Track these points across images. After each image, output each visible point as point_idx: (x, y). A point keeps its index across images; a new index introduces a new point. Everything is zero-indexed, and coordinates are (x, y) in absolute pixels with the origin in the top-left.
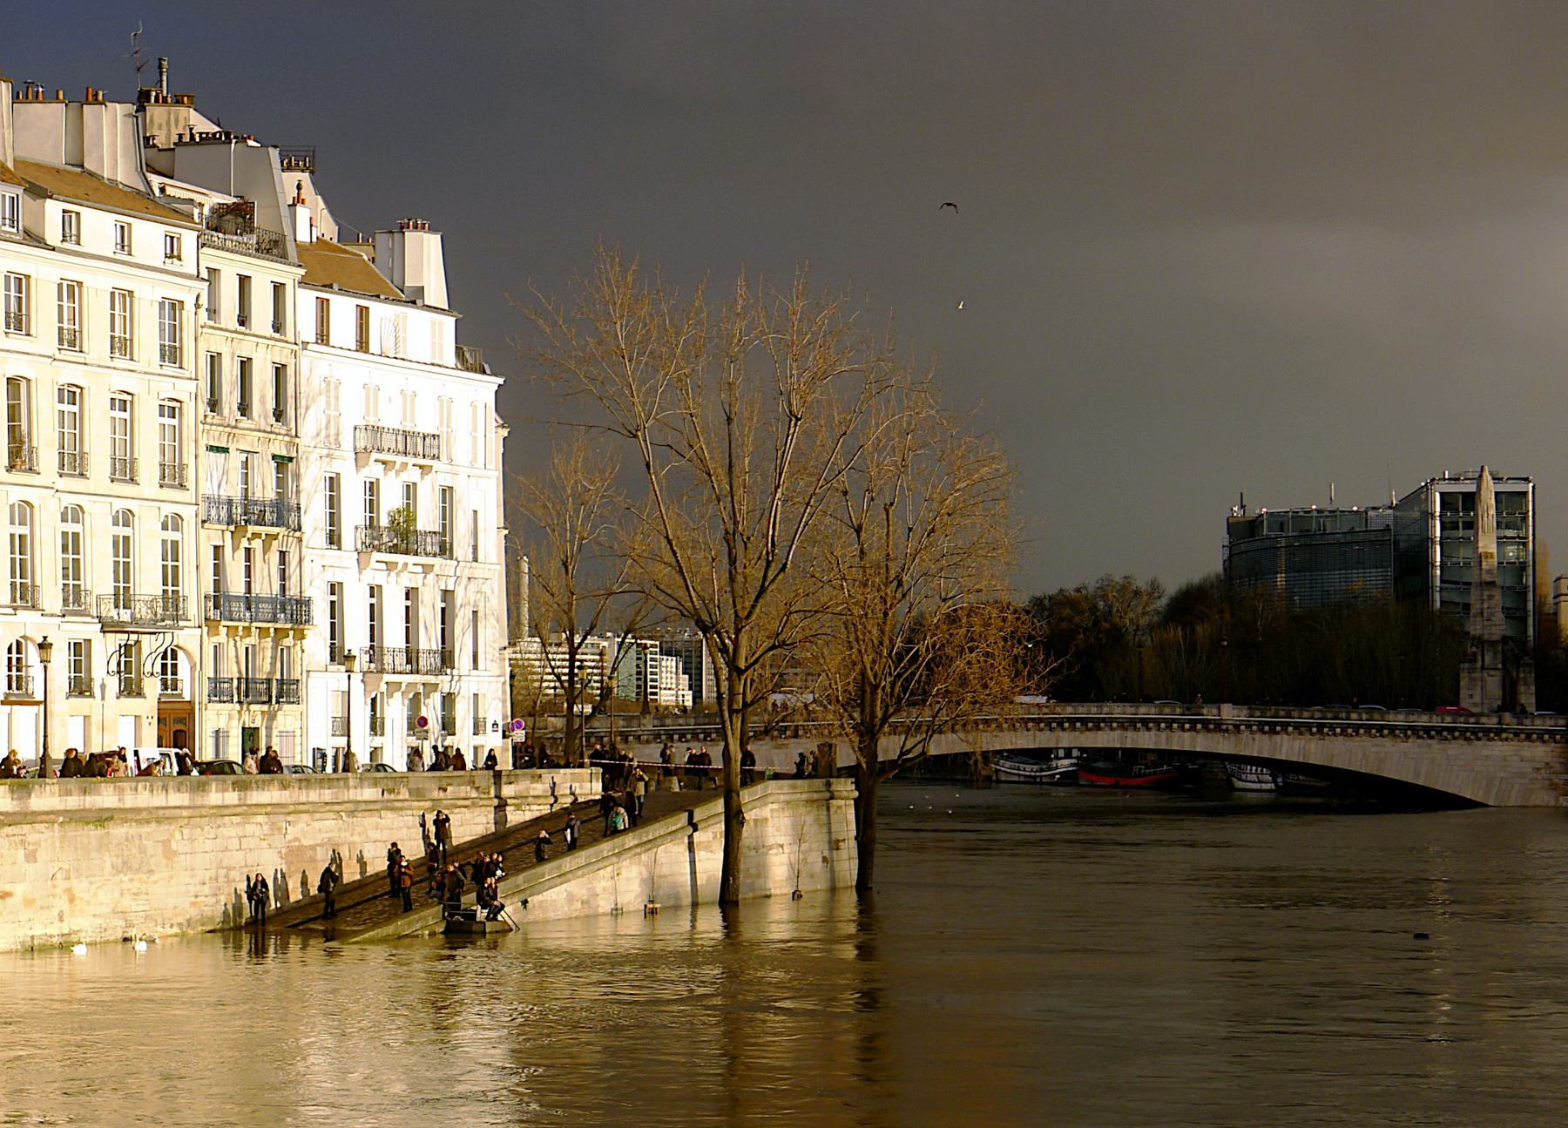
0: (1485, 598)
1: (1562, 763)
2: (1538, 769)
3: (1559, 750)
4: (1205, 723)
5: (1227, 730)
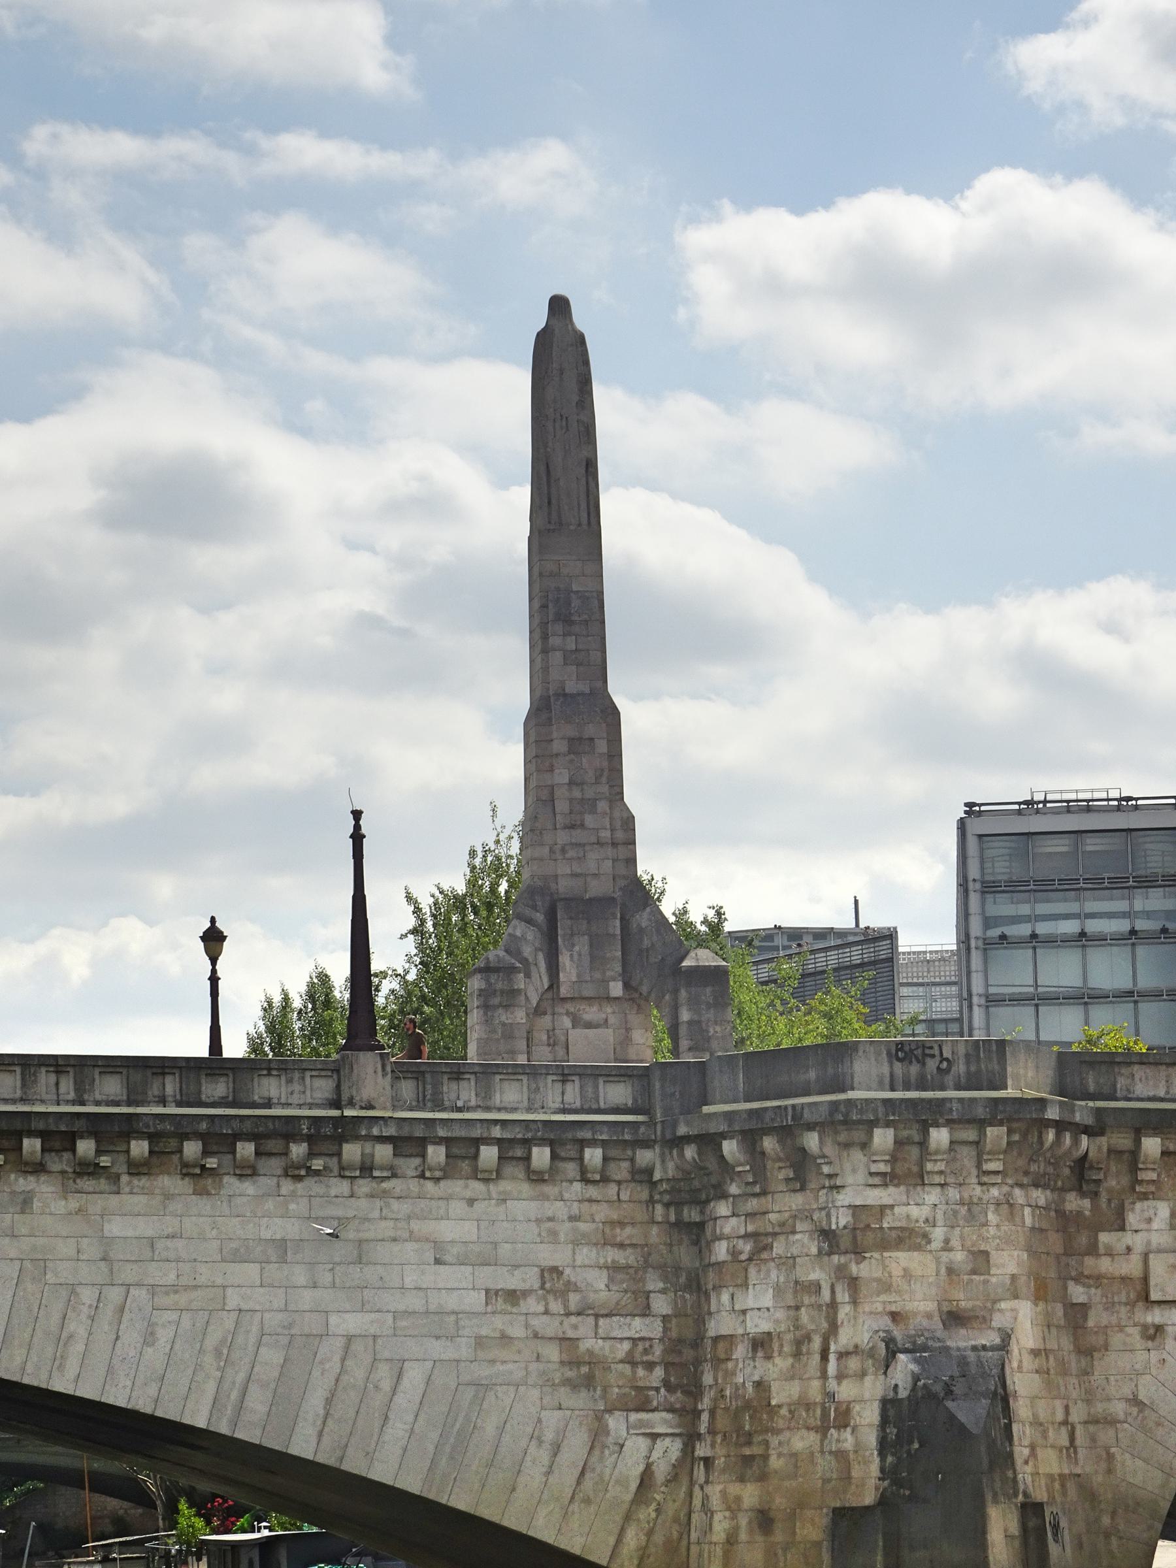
0: (559, 746)
1: (614, 1269)
2: (513, 1296)
3: (602, 1212)
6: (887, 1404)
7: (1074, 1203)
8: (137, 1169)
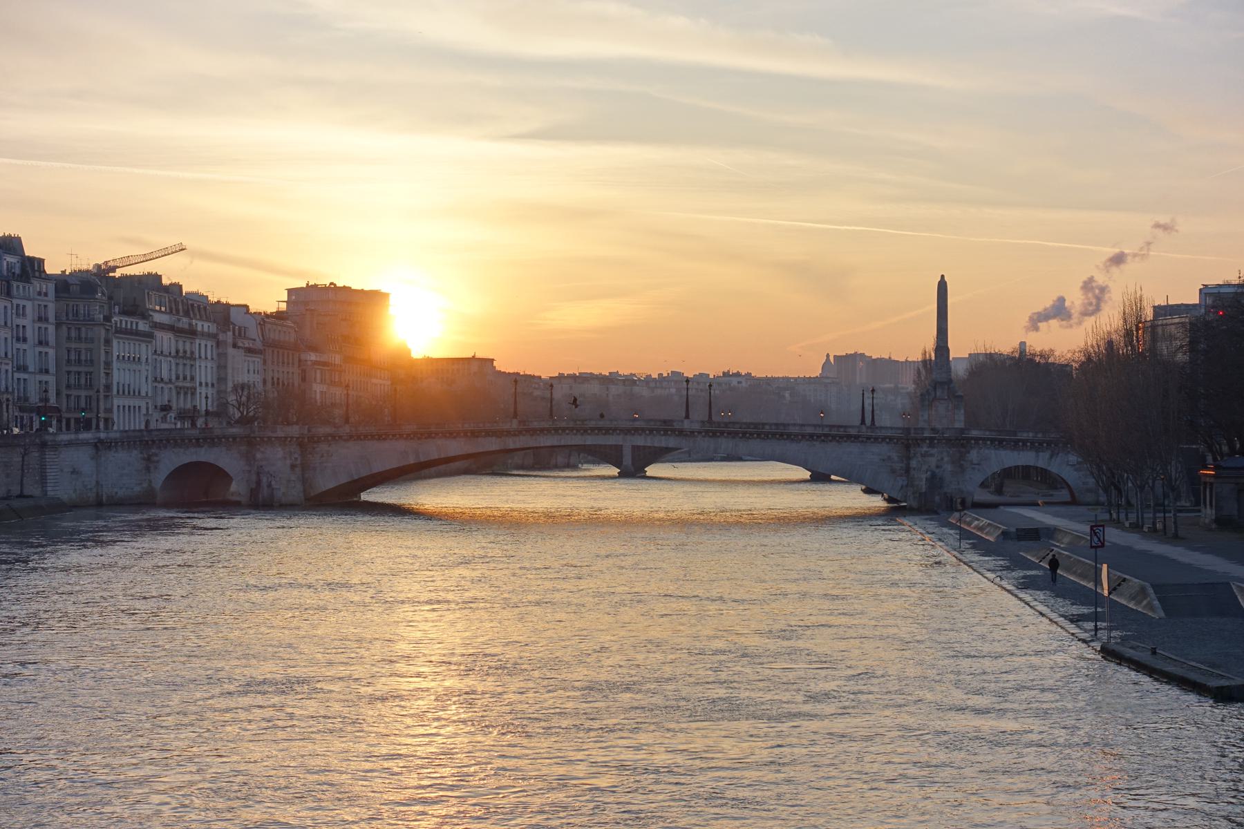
4: (673, 431)
5: (686, 435)
6: (926, 479)
7: (963, 450)
8: (830, 441)
